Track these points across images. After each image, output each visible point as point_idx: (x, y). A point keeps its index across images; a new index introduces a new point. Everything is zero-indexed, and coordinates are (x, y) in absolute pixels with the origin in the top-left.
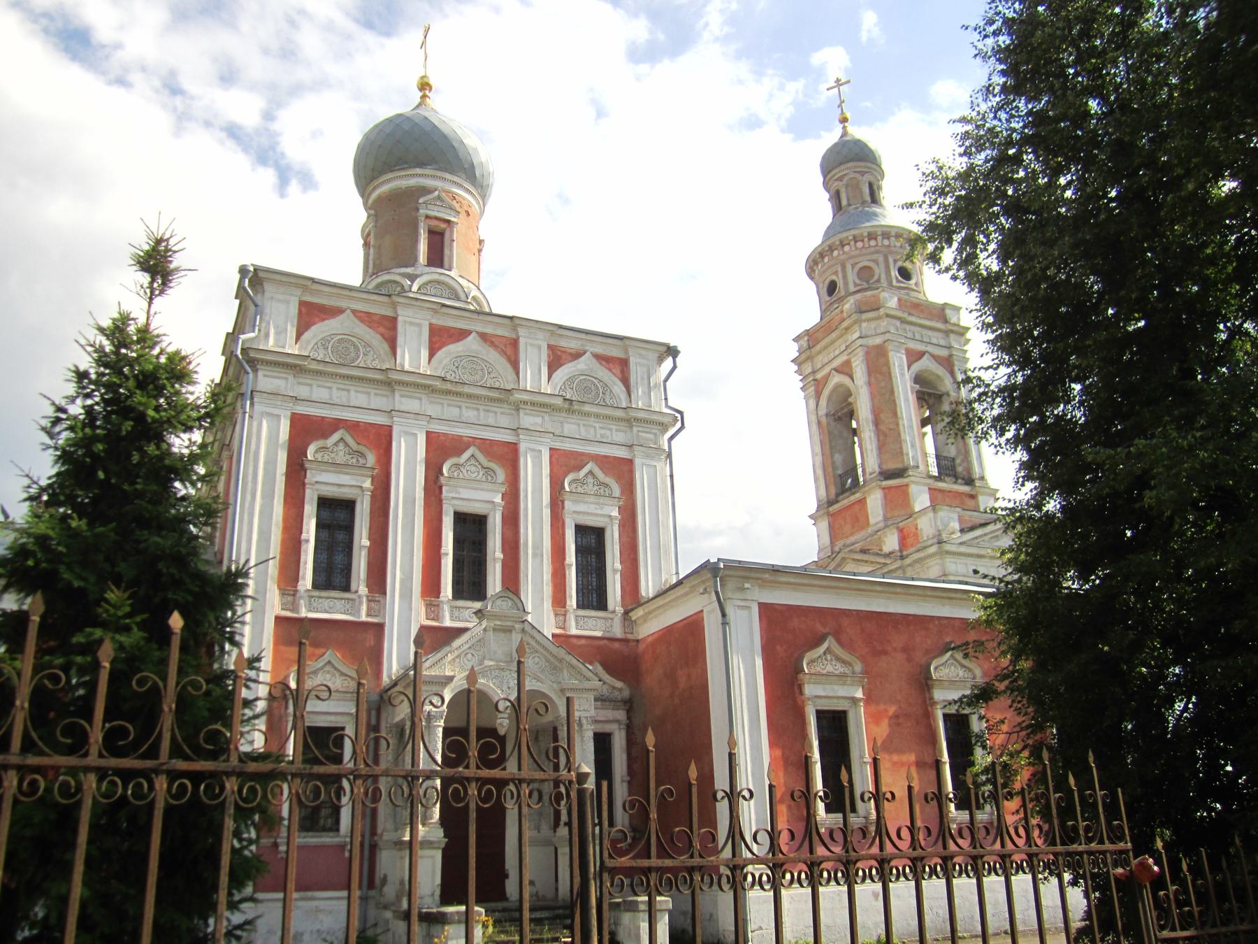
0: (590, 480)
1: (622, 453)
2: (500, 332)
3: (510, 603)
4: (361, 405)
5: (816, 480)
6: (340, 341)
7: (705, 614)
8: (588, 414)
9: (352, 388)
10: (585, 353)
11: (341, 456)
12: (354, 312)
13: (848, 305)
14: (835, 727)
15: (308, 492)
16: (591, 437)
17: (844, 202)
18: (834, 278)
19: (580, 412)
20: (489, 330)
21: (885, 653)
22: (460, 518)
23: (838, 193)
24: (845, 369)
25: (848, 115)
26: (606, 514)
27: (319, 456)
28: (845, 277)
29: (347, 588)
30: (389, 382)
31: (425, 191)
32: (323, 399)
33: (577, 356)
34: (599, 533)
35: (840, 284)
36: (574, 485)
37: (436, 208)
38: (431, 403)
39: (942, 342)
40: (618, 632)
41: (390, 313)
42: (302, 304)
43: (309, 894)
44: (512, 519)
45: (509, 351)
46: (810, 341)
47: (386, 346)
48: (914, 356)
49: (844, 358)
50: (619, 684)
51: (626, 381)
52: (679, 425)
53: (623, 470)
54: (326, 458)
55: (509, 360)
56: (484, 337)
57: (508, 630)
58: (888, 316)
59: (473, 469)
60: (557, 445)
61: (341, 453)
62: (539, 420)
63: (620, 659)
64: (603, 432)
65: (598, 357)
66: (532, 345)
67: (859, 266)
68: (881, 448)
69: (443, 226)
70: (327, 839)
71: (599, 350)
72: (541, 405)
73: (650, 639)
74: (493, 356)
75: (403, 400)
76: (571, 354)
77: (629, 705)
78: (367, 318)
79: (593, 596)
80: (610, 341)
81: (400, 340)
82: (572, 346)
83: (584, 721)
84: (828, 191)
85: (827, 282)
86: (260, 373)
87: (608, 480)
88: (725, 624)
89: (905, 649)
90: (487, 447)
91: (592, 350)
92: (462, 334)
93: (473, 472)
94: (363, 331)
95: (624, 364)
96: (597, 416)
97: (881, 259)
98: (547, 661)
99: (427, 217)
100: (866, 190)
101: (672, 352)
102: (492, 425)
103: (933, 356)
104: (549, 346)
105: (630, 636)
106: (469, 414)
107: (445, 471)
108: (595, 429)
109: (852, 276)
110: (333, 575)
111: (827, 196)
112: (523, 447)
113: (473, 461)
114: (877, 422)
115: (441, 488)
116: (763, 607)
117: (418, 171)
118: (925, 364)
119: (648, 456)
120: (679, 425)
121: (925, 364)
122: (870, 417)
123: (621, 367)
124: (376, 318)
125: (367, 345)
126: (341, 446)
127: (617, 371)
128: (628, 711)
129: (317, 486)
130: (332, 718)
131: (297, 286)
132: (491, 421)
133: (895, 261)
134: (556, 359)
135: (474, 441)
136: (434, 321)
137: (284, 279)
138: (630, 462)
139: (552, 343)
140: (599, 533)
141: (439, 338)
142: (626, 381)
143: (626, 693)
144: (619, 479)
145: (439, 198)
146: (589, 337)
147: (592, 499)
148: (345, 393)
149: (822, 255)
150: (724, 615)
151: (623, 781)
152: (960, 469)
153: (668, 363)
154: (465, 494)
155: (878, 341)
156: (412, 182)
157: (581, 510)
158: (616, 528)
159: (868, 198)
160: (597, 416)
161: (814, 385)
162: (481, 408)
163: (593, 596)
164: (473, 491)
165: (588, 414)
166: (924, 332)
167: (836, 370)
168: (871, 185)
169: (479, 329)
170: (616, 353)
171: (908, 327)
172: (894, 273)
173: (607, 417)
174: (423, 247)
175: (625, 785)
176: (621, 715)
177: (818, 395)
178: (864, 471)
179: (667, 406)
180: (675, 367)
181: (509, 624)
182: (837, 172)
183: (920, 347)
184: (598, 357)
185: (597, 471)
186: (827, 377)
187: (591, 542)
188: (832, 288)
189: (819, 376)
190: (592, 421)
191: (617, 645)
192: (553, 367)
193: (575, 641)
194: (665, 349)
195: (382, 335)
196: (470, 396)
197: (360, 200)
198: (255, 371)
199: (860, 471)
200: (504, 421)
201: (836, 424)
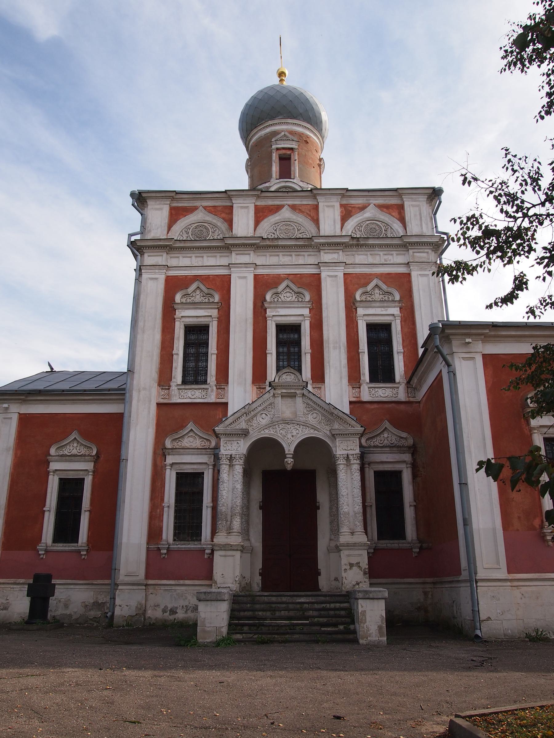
0: (377, 291)
1: (402, 270)
2: (305, 202)
3: (293, 376)
4: (210, 264)
6: (196, 227)
8: (373, 246)
9: (205, 255)
10: (369, 205)
11: (198, 298)
15: (177, 324)
19: (366, 245)
20: (297, 202)
26: (390, 314)
27: (184, 300)
29: (205, 382)
30: (227, 246)
32: (186, 264)
33: (363, 208)
34: (387, 327)
36: (365, 297)
38: (258, 256)
40: (401, 395)
41: (228, 204)
43: (181, 582)
44: (317, 325)
45: (313, 214)
47: (226, 225)
50: (404, 435)
51: (402, 220)
54: (188, 301)
56: (293, 208)
57: (293, 396)
59: (288, 294)
60: (350, 271)
61: (198, 297)
62: (335, 256)
64: (386, 257)
66: (328, 206)
69: (289, 152)
70: (192, 546)
71: (381, 201)
72: (335, 244)
73: (425, 398)
75: (238, 256)
76: (359, 208)
77: (413, 450)
79: (382, 371)
80: (387, 193)
82: (360, 202)
87: (390, 290)
91: (375, 202)
93: (288, 296)
94: (210, 218)
95: (400, 208)
96: (380, 246)
98: (323, 415)
99: (278, 149)
102: (301, 263)
104: (341, 206)
106: (285, 260)
107: (268, 297)
108: (381, 257)
110: (194, 375)
113: (288, 290)
115: (265, 310)
117: (270, 122)
119: (421, 269)
120: (446, 243)
124: (220, 209)
125: (215, 226)
126: (198, 292)
127: (396, 214)
128: (413, 454)
129: (183, 319)
130: (195, 467)
132: (301, 262)
134: (347, 213)
136: (259, 203)
139: (344, 202)
140: (387, 327)
143: (411, 442)
144: (399, 288)
146: (371, 194)
147: (378, 304)
148: (201, 259)
151: (410, 506)
154: (282, 312)
156: (268, 130)
158: (398, 321)
160: (380, 246)
162: (293, 254)
163: (382, 371)
164: (289, 310)
165: (373, 246)
169: (290, 202)
170: (394, 201)
173: (388, 246)
174: (275, 169)
175: (412, 508)
176: (407, 457)
181: (293, 391)
185: (381, 284)
190: (377, 251)
191: (402, 407)
192: (344, 219)
193: (368, 406)
195: (223, 219)
196: (284, 247)
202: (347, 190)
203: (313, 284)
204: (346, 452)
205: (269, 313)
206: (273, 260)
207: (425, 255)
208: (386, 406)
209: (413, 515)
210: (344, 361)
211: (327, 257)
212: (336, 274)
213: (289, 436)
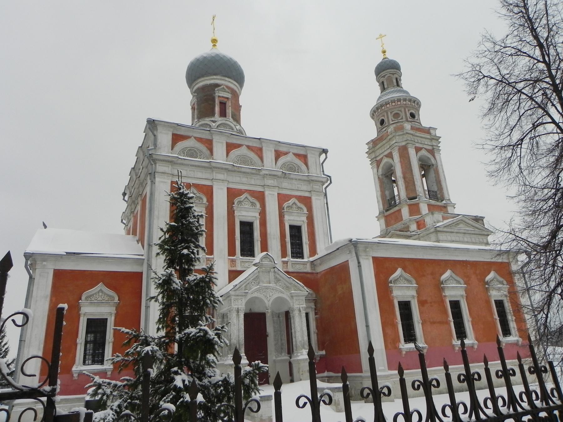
0: (294, 206)
1: (307, 194)
2: (255, 145)
5: (378, 202)
6: (189, 150)
7: (349, 262)
12: (195, 138)
13: (391, 129)
14: (405, 307)
16: (293, 188)
17: (386, 87)
18: (383, 118)
20: (250, 144)
21: (424, 276)
22: (242, 224)
23: (383, 82)
24: (390, 156)
25: (385, 49)
26: (300, 219)
28: (388, 117)
30: (211, 168)
31: (217, 85)
33: (286, 154)
35: (386, 120)
37: (223, 93)
39: (429, 144)
41: (210, 138)
42: (174, 135)
44: (263, 223)
46: (374, 144)
48: (418, 150)
49: (389, 151)
51: (306, 164)
52: (329, 182)
53: (307, 201)
55: (259, 156)
56: (248, 147)
58: (407, 133)
59: (247, 203)
60: (281, 192)
62: (272, 181)
63: (308, 280)
64: (299, 186)
65: (296, 155)
67: (394, 113)
68: (407, 188)
69: (226, 100)
71: (295, 151)
73: (323, 272)
74: (252, 155)
75: (217, 174)
78: (200, 140)
81: (215, 149)
83: (301, 309)
84: (379, 82)
85: (380, 120)
86: (157, 165)
88: (359, 266)
89: (432, 274)
90: (252, 193)
92: (239, 146)
93: (247, 205)
94: (199, 145)
97: (403, 110)
99: (219, 96)
100: (395, 81)
101: (325, 151)
103: (425, 149)
104: (275, 151)
105: (314, 271)
106: (244, 180)
109: (391, 117)
111: (378, 84)
112: (267, 193)
113: (246, 200)
114: (404, 178)
115: (234, 211)
116: (375, 259)
117: (215, 77)
118: (423, 153)
121: (423, 153)
122: (402, 175)
123: (304, 158)
125: (201, 151)
131: (171, 127)
133: (409, 110)
134: (278, 155)
135: (246, 191)
136: (228, 141)
137: (166, 124)
138: (310, 198)
141: (230, 147)
142: (306, 164)
145: (223, 88)
147: (296, 214)
149: (378, 109)
150: (359, 263)
151: (314, 333)
152: (439, 196)
153: (323, 156)
154: (244, 213)
155: (404, 144)
156: (212, 82)
157: (291, 219)
158: (306, 225)
159: (395, 84)
161: (376, 162)
164: (247, 212)
166: (422, 139)
167: (385, 156)
168: (397, 79)
169: (247, 144)
170: (302, 152)
171: (415, 138)
172: (408, 115)
174: (217, 109)
175: (316, 335)
177: (378, 167)
178: (399, 198)
179: (324, 174)
180: (326, 158)
182: (383, 74)
183: (421, 146)
184: (296, 155)
185: (297, 202)
186: (382, 159)
187: (296, 231)
188: (382, 122)
189: (378, 159)
191: (309, 276)
192: (277, 159)
194: (322, 150)
195: (207, 147)
196: (244, 173)
197: (189, 90)
198: (155, 164)
199: (397, 198)
200: (258, 182)
201: (386, 178)
202: (279, 142)
203: (260, 197)
204: (298, 306)
205: (236, 213)
206: (237, 179)
207: (318, 187)
208: (301, 275)
209: (316, 338)
210: (279, 247)
211: (270, 182)
212: (273, 193)
213: (268, 296)
